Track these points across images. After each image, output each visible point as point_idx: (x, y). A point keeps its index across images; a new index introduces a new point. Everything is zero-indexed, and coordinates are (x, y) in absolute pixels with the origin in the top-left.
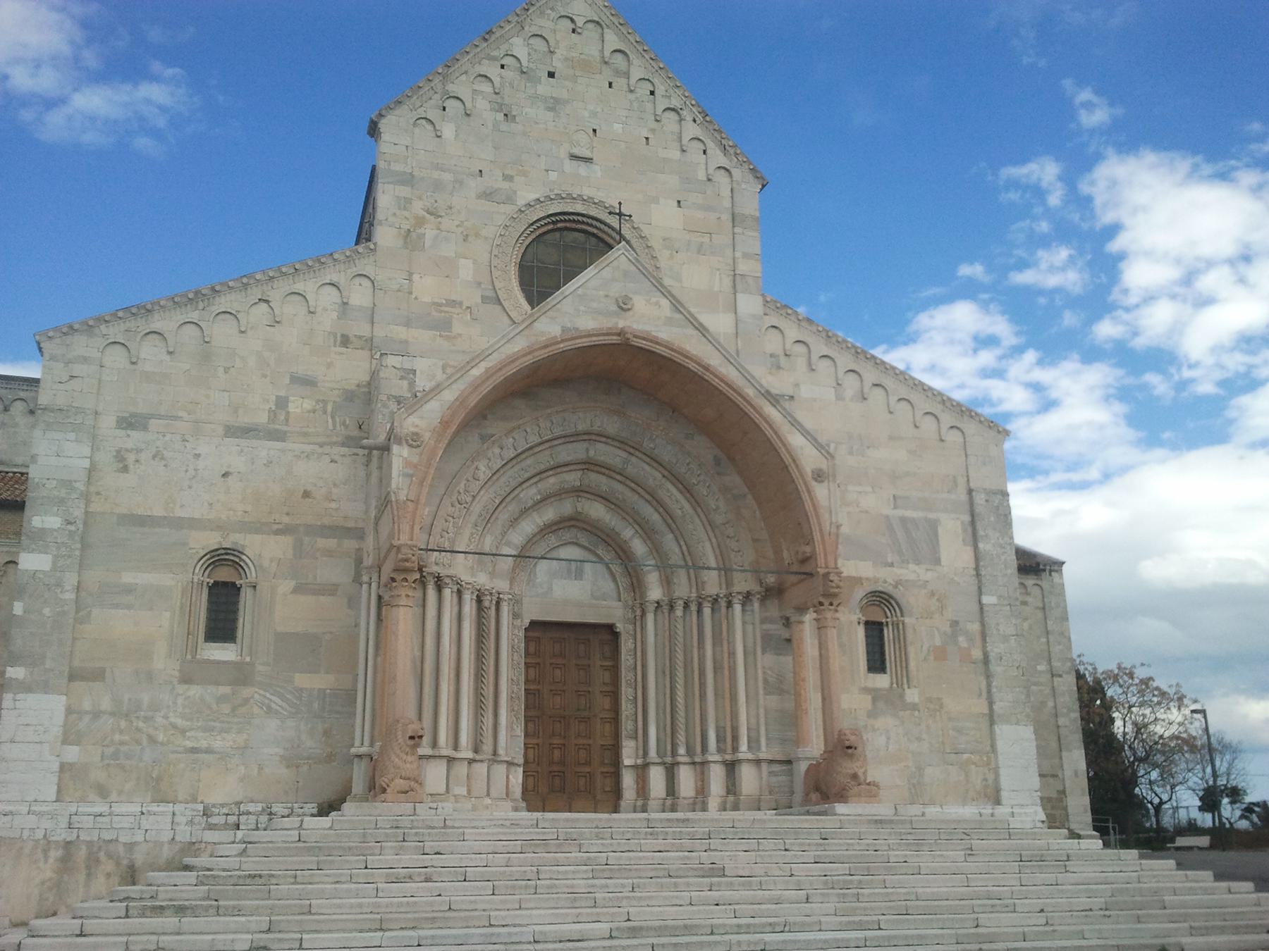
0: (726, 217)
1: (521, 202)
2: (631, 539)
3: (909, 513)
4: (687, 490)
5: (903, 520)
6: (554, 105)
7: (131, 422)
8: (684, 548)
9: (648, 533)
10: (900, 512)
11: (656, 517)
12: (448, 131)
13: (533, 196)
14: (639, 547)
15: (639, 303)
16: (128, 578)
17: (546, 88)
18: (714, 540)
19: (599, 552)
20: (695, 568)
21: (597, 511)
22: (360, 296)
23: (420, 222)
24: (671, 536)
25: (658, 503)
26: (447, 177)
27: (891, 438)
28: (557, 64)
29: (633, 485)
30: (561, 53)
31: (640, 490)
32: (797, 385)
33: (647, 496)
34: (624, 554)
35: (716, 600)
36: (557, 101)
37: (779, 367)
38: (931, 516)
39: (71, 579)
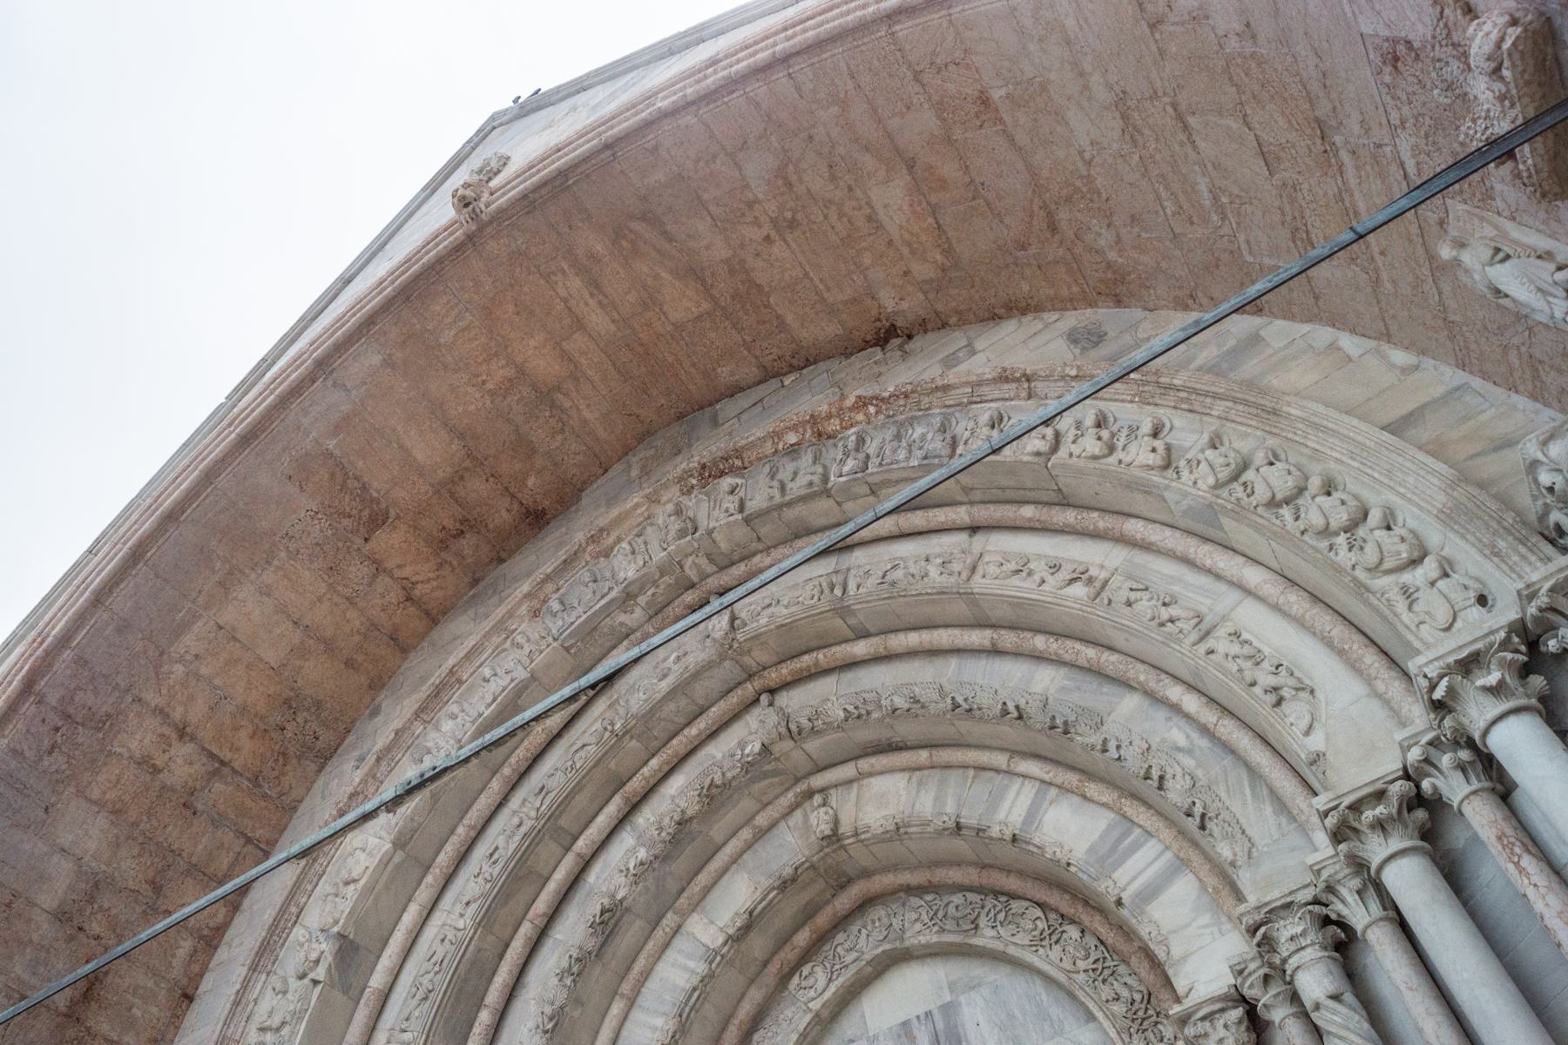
2: (1032, 815)
4: (1053, 501)
8: (1191, 703)
9: (1056, 748)
11: (1045, 680)
14: (1070, 829)
18: (1254, 576)
19: (986, 938)
20: (1245, 717)
21: (884, 800)
24: (1130, 703)
25: (1012, 628)
29: (913, 639)
31: (943, 637)
33: (977, 638)
34: (1064, 898)
35: (1417, 800)
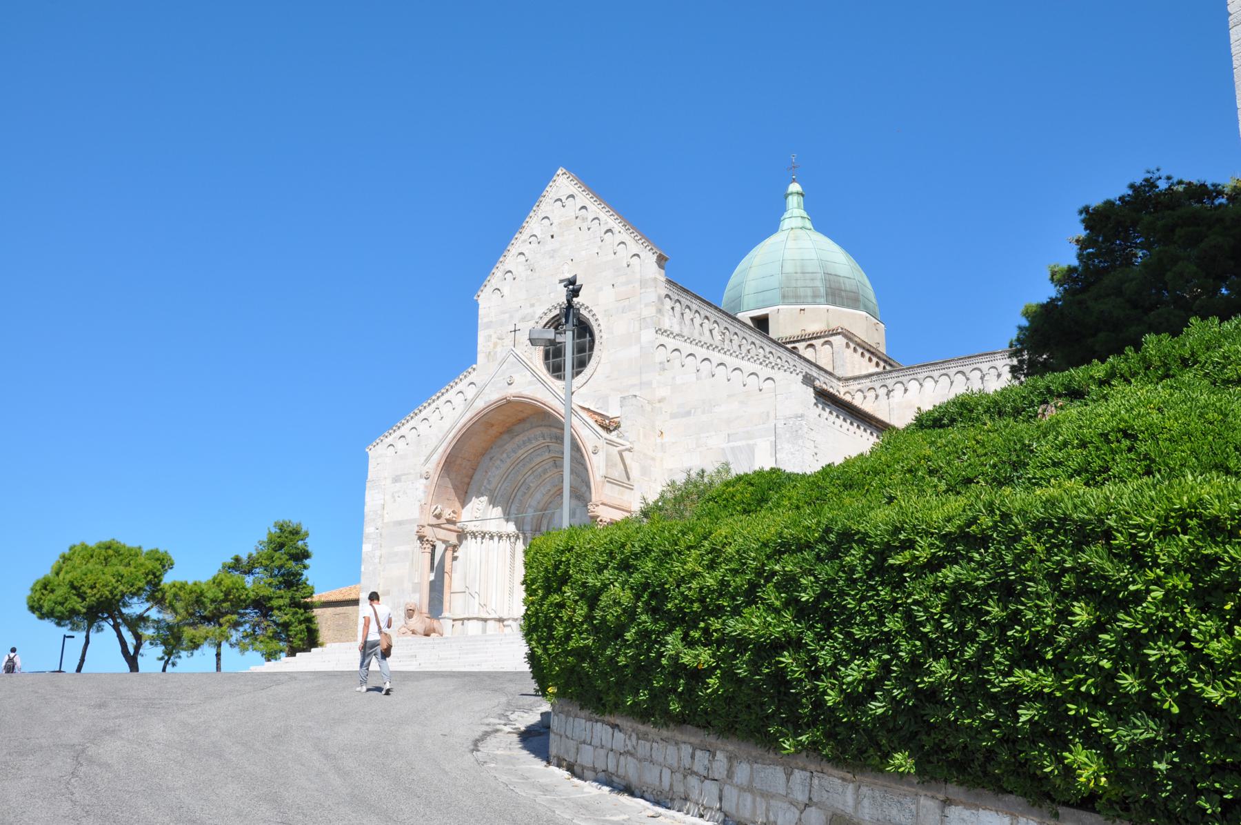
0: (637, 285)
1: (537, 316)
3: (736, 444)
5: (732, 449)
6: (552, 254)
7: (396, 479)
10: (731, 444)
12: (506, 290)
13: (539, 313)
15: (517, 378)
16: (396, 549)
17: (550, 245)
22: (470, 392)
23: (495, 345)
26: (507, 315)
27: (729, 396)
28: (554, 230)
30: (556, 222)
32: (674, 378)
36: (554, 251)
37: (664, 369)
38: (751, 442)
39: (378, 553)
